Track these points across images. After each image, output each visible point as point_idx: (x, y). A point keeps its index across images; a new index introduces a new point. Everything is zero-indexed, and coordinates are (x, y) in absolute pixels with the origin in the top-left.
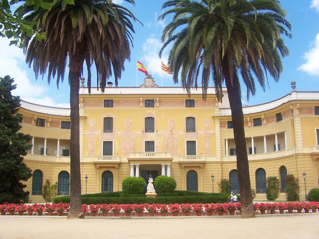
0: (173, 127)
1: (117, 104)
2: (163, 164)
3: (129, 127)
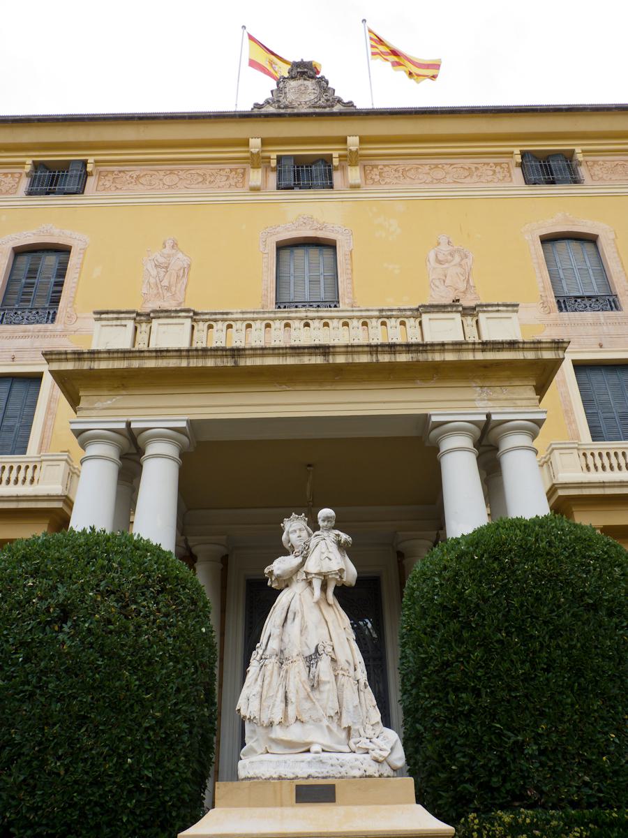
0: (462, 286)
1: (108, 184)
2: (454, 408)
3: (168, 288)
